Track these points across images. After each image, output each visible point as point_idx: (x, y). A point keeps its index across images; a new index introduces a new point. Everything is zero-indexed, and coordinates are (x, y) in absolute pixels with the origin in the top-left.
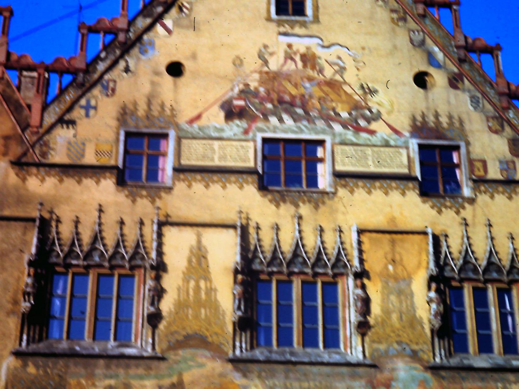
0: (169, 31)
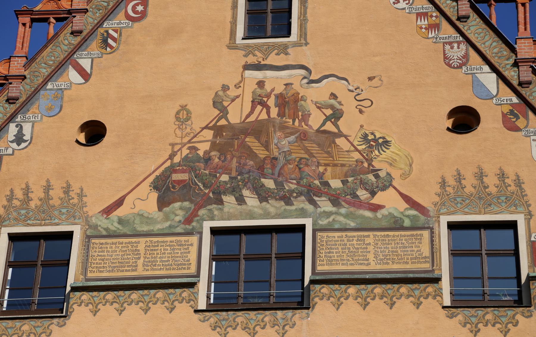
0: (86, 76)
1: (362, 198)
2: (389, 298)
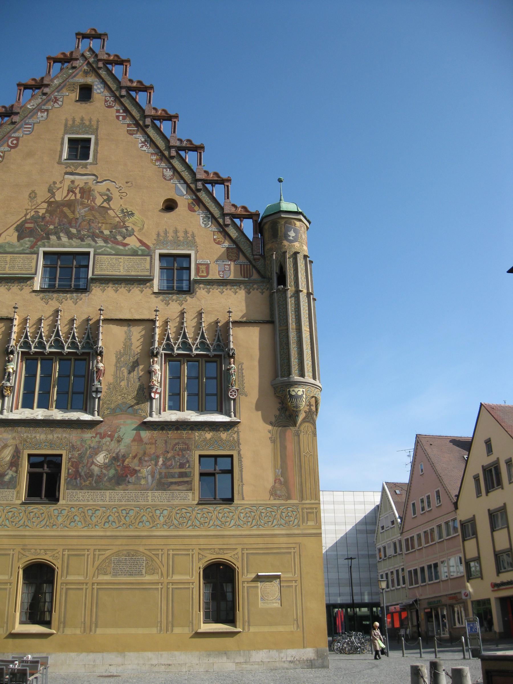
1: (119, 240)
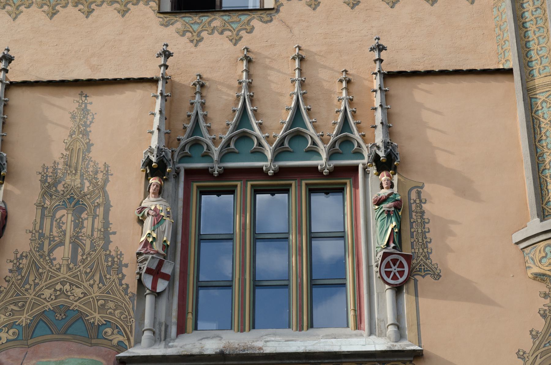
2: (86, 5)
